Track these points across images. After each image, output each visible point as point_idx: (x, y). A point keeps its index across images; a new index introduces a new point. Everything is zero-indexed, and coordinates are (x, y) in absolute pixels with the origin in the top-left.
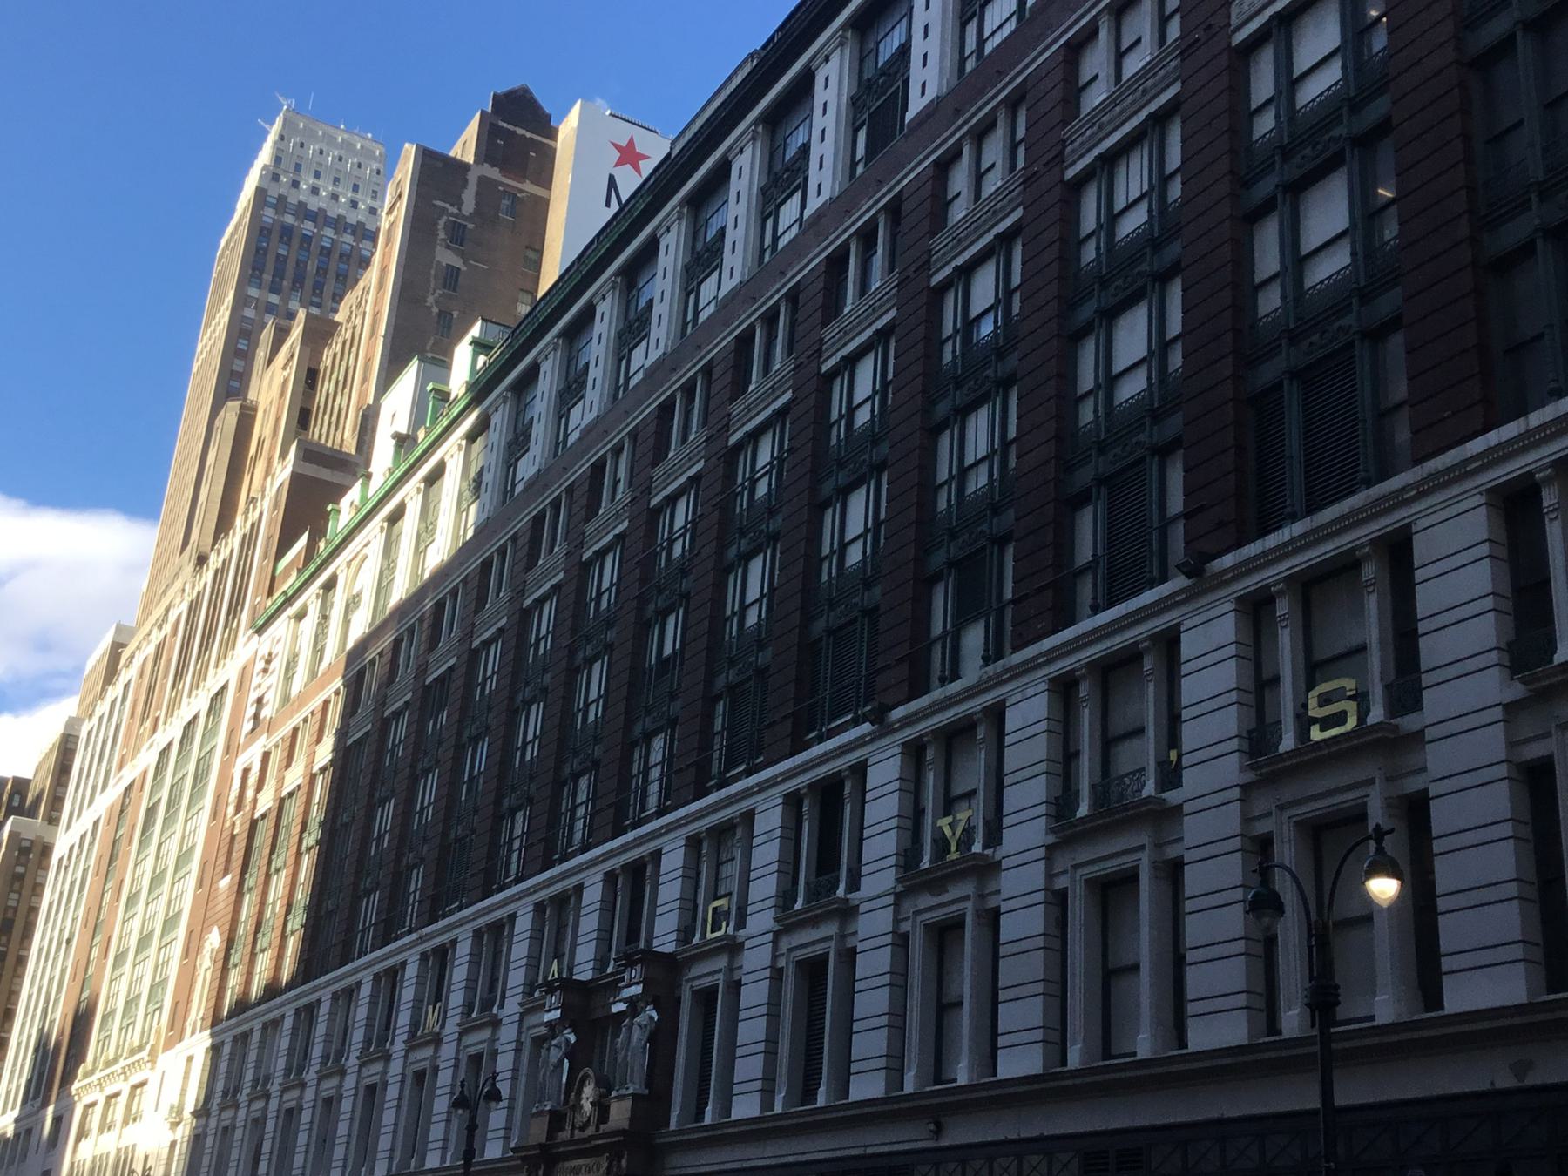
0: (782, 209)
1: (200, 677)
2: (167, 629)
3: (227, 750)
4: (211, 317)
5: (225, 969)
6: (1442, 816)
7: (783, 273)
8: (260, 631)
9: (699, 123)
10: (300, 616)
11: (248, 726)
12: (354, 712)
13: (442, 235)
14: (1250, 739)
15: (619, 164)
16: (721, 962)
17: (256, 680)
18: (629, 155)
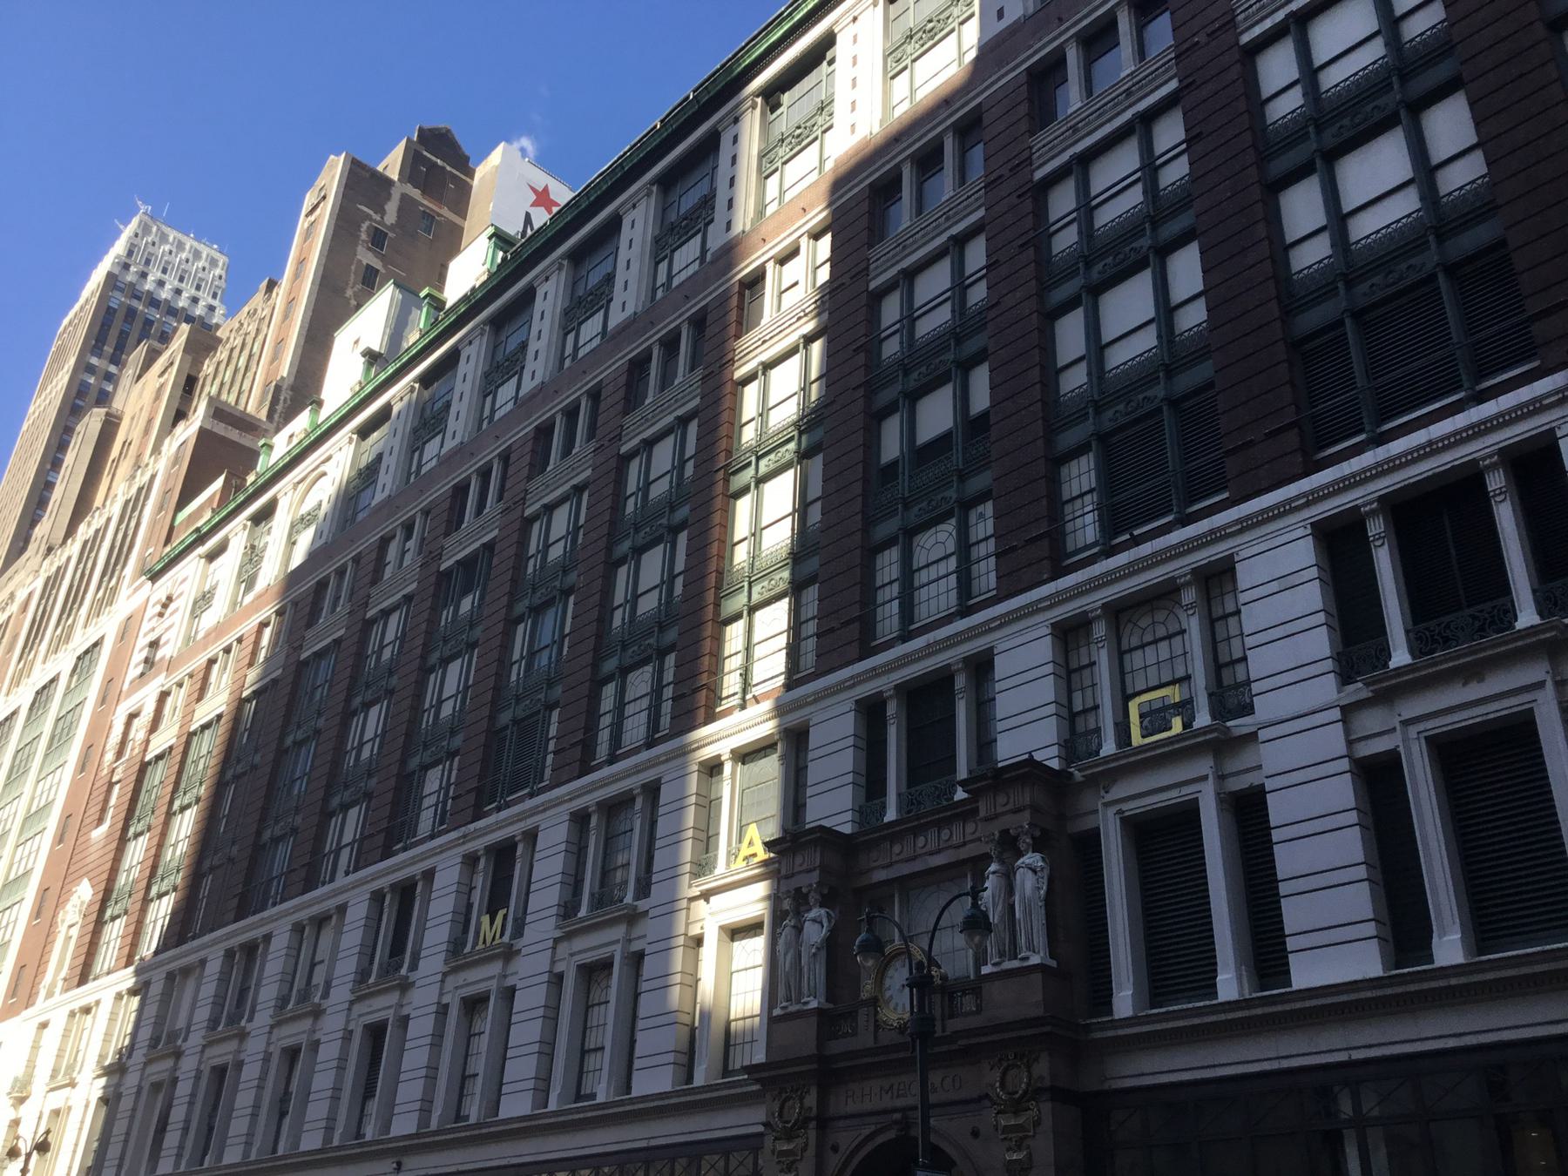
1: (66, 637)
2: (14, 608)
3: (103, 699)
4: (49, 379)
5: (99, 924)
8: (154, 577)
10: (211, 557)
11: (134, 671)
13: (364, 236)
16: (495, 968)
17: (146, 627)
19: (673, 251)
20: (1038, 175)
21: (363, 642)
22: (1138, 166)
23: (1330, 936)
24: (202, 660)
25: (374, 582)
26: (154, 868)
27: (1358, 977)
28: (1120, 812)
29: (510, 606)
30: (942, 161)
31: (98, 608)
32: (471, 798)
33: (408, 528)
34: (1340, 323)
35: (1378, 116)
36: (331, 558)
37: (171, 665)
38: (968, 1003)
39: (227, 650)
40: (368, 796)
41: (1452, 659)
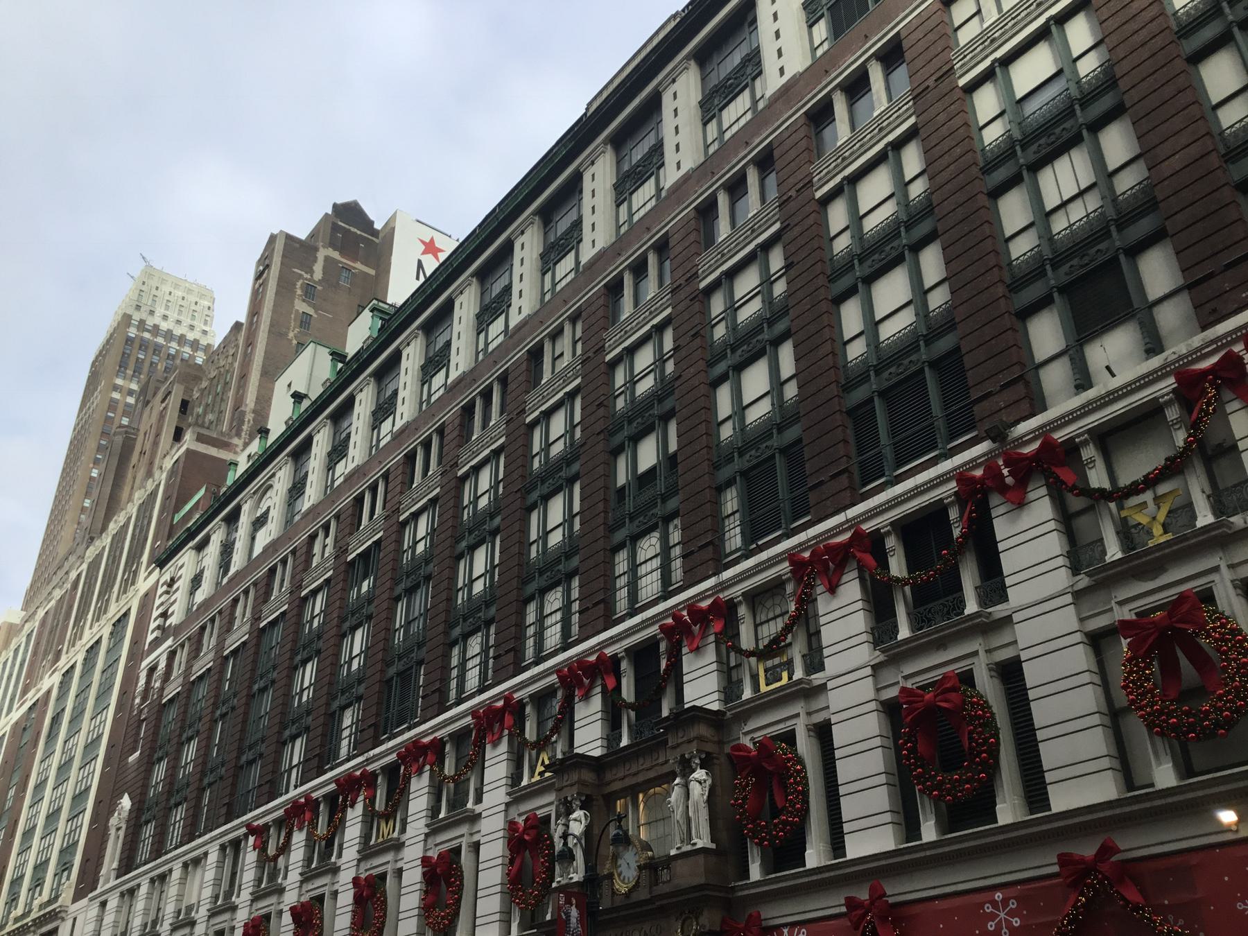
0: (558, 266)
6: (1032, 674)
7: (648, 229)
8: (161, 563)
9: (661, 36)
10: (200, 548)
12: (266, 601)
14: (873, 634)
15: (423, 253)
18: (430, 248)
19: (488, 325)
20: (703, 285)
21: (300, 615)
22: (758, 283)
23: (1077, 772)
24: (196, 628)
25: (305, 570)
26: (171, 784)
27: (1083, 804)
28: (752, 739)
29: (291, 659)
30: (647, 270)
31: (124, 590)
32: (371, 731)
33: (326, 528)
34: (871, 400)
35: (1066, 136)
36: (290, 539)
37: (177, 630)
38: (665, 875)
39: (213, 620)
40: (307, 729)
41: (938, 632)
